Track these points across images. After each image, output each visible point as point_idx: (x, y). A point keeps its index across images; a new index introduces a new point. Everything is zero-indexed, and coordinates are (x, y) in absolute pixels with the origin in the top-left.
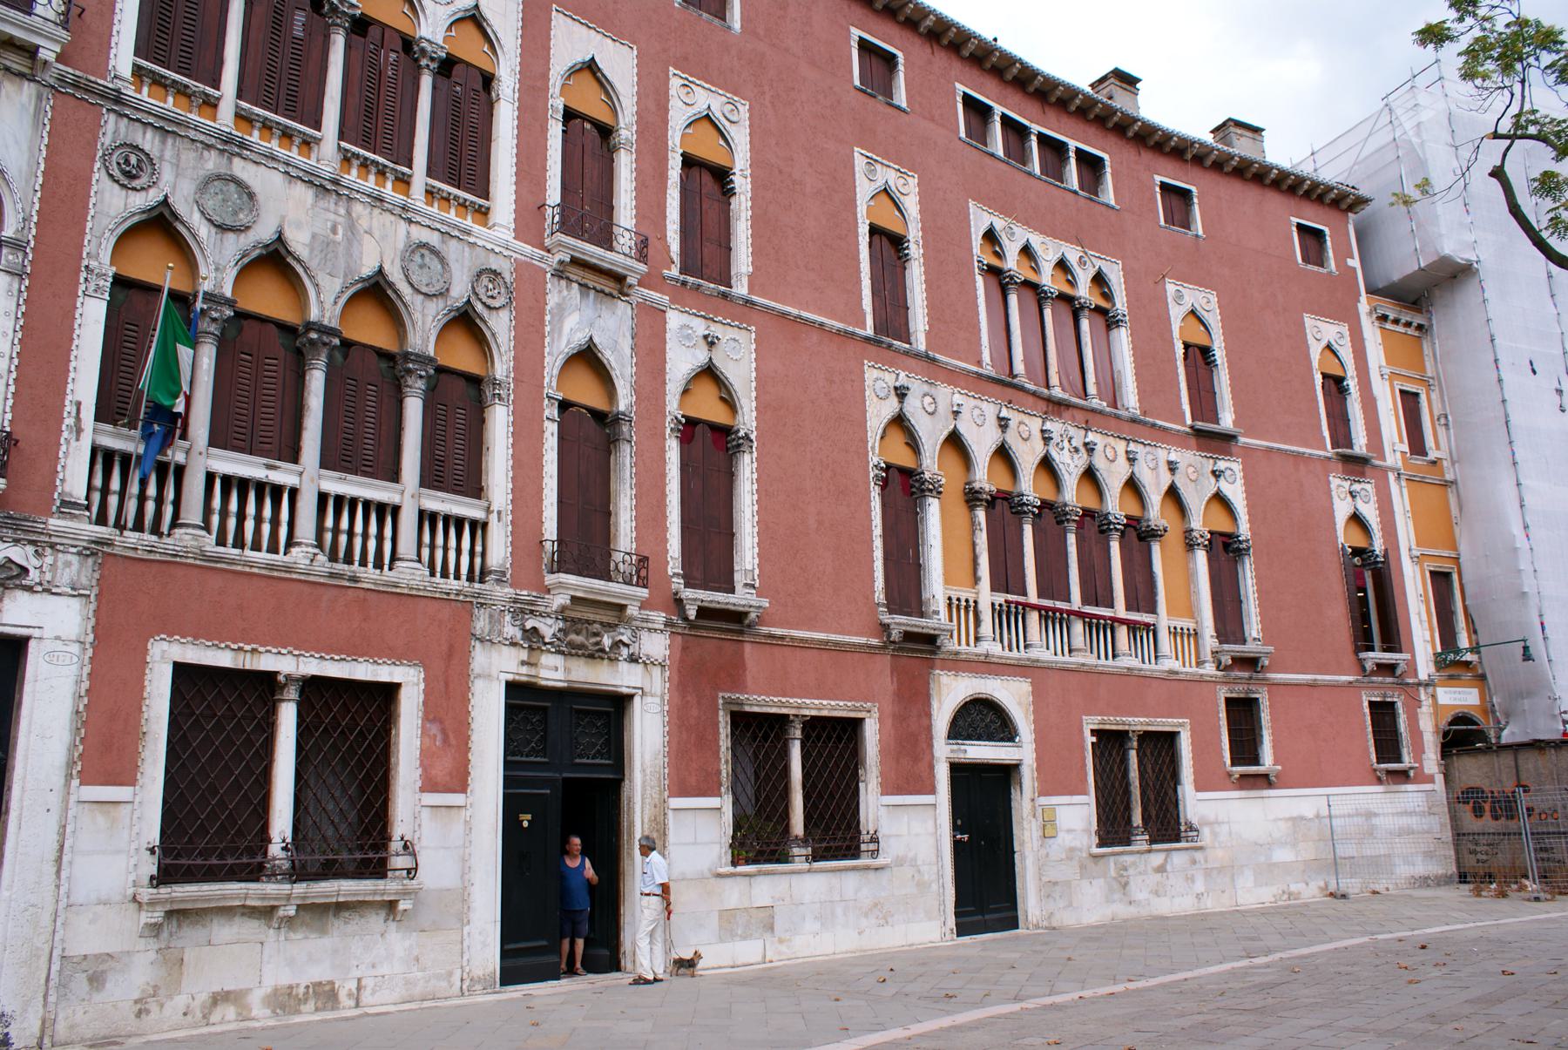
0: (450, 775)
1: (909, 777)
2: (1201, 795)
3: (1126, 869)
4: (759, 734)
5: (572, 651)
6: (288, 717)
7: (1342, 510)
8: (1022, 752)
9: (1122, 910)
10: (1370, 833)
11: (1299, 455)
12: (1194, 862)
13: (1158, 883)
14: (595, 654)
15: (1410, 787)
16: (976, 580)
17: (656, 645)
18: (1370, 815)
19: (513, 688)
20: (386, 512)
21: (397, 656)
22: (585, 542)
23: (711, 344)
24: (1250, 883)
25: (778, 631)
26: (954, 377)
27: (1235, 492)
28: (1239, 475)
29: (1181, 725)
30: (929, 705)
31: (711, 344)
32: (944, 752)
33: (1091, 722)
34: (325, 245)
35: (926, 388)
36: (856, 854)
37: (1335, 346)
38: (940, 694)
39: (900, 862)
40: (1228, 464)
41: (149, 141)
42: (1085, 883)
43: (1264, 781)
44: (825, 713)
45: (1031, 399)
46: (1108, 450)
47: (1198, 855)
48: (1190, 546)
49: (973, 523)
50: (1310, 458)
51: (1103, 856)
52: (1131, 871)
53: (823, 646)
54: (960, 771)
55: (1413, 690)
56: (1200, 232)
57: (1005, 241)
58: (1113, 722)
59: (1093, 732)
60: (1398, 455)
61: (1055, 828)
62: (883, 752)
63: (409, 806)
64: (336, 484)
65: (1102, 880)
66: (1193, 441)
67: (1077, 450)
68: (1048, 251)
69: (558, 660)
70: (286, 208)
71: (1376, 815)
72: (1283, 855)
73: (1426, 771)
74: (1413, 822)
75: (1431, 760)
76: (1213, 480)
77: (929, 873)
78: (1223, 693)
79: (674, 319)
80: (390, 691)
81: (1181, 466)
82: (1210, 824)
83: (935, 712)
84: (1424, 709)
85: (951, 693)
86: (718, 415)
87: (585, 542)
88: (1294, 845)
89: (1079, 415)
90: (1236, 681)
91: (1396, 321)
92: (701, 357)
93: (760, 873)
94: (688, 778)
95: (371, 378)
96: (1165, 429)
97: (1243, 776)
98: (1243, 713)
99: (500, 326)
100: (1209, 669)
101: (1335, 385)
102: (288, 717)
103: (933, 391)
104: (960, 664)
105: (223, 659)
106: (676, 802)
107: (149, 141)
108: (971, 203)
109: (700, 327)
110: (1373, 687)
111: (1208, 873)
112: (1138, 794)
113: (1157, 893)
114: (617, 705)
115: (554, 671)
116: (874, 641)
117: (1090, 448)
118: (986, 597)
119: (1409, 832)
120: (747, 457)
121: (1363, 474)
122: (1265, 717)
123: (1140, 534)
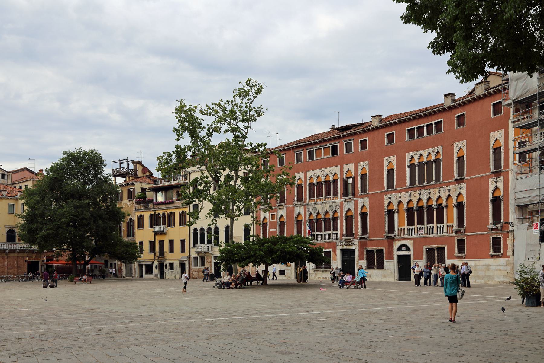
0: (335, 259)
1: (391, 257)
4: (370, 253)
5: (347, 245)
7: (492, 187)
8: (411, 253)
14: (349, 245)
17: (357, 243)
20: (330, 234)
21: (330, 248)
22: (349, 233)
26: (400, 191)
32: (396, 253)
34: (322, 210)
41: (309, 207)
50: (484, 176)
54: (399, 257)
57: (415, 157)
58: (430, 246)
64: (326, 233)
68: (424, 153)
70: (319, 208)
79: (359, 200)
85: (397, 244)
87: (349, 233)
89: (428, 187)
90: (459, 236)
91: (523, 119)
95: (326, 220)
98: (461, 243)
99: (338, 211)
100: (453, 234)
104: (398, 240)
107: (309, 207)
109: (362, 200)
114: (353, 251)
115: (345, 247)
118: (406, 227)
123: (440, 208)
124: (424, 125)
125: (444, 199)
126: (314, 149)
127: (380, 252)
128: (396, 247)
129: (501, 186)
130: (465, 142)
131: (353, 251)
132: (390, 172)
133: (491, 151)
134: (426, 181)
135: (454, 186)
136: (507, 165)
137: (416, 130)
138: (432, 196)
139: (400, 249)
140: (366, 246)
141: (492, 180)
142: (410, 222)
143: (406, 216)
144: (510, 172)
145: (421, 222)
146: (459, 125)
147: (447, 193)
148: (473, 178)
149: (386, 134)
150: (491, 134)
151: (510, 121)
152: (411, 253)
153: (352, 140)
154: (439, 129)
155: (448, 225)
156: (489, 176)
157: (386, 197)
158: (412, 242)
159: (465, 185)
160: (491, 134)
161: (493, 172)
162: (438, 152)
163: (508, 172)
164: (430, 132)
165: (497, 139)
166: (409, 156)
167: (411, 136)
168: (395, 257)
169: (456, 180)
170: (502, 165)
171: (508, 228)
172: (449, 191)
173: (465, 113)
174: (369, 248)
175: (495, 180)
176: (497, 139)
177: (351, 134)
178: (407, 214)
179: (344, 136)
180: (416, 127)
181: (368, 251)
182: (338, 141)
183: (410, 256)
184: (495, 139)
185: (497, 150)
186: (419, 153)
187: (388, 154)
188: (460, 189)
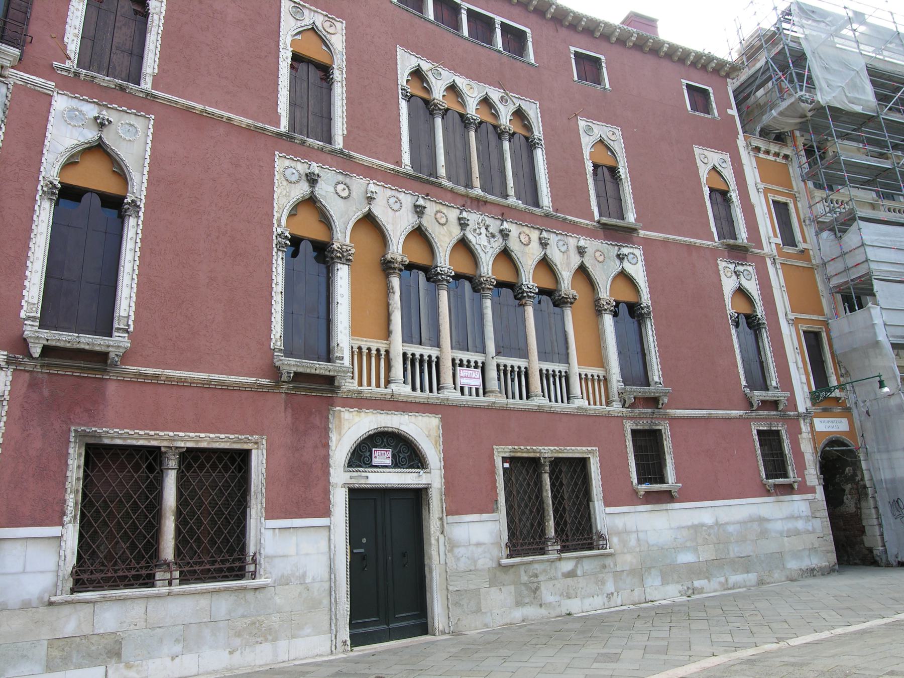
2: (609, 510)
3: (536, 576)
7: (729, 285)
8: (432, 478)
9: (531, 612)
10: (764, 534)
12: (604, 567)
13: (567, 586)
15: (795, 497)
16: (388, 334)
18: (762, 520)
23: (102, 125)
24: (657, 582)
25: (150, 371)
26: (369, 172)
27: (638, 271)
28: (641, 258)
29: (590, 452)
30: (327, 437)
31: (102, 125)
32: (341, 479)
33: (501, 452)
35: (340, 178)
36: (238, 573)
37: (719, 168)
38: (339, 428)
39: (284, 581)
40: (631, 250)
42: (494, 590)
43: (667, 497)
44: (204, 445)
45: (449, 195)
46: (522, 237)
47: (609, 561)
48: (599, 311)
49: (388, 290)
50: (699, 248)
51: (512, 566)
52: (541, 578)
53: (206, 386)
54: (359, 497)
55: (794, 422)
56: (608, 86)
58: (525, 451)
59: (504, 459)
60: (773, 246)
61: (466, 542)
62: (271, 478)
65: (512, 588)
66: (601, 232)
67: (493, 236)
71: (768, 520)
72: (686, 558)
73: (808, 484)
74: (800, 525)
75: (813, 476)
76: (618, 262)
77: (319, 589)
78: (629, 426)
79: (61, 103)
81: (590, 251)
82: (618, 533)
83: (333, 444)
84: (804, 435)
85: (351, 427)
86: (103, 182)
88: (695, 550)
92: (90, 135)
93: (104, 600)
97: (647, 493)
100: (616, 407)
101: (721, 196)
103: (348, 181)
104: (360, 402)
108: (400, 51)
109: (91, 110)
110: (758, 419)
111: (617, 575)
112: (550, 509)
113: (569, 597)
116: (264, 381)
117: (505, 234)
118: (398, 347)
119: (797, 533)
120: (132, 222)
121: (745, 259)
122: (668, 444)
128: (341, 447)
139: (360, 457)
140: (93, 417)
148: (665, 242)
152: (432, 478)
158: (432, 422)
168: (339, 500)
174: (118, 435)
181: (97, 454)
188: (621, 257)
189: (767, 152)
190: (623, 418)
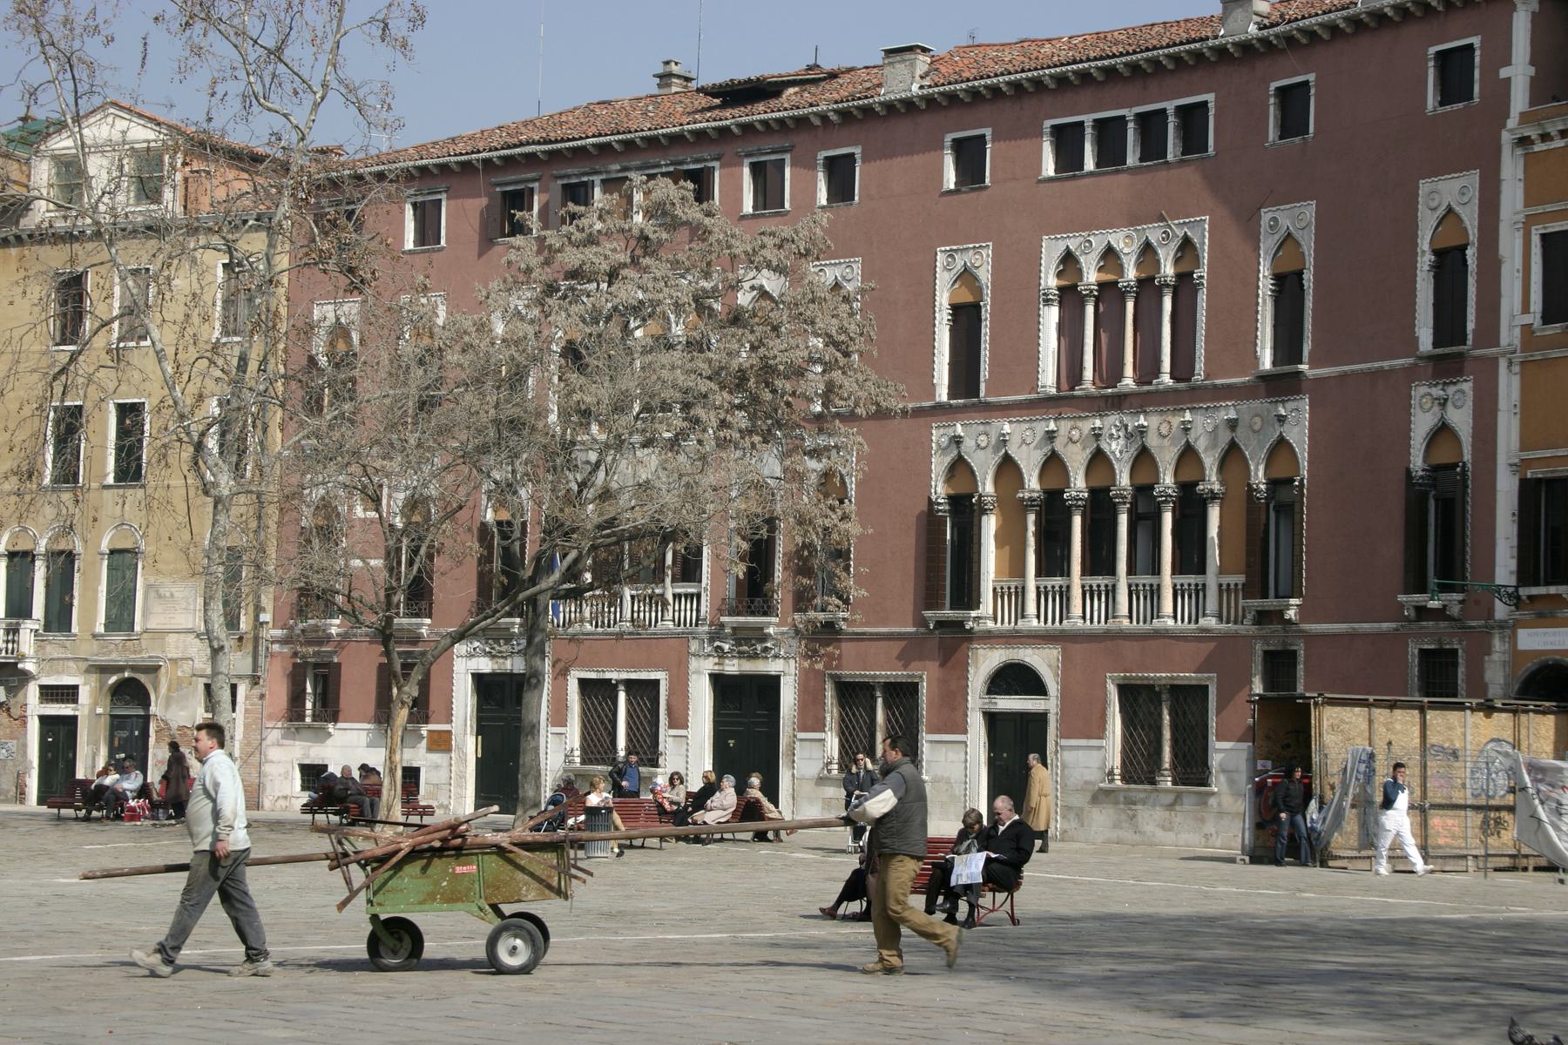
0: (679, 721)
4: (853, 695)
6: (622, 696)
7: (1422, 424)
8: (1049, 704)
11: (1380, 371)
14: (754, 656)
19: (711, 675)
26: (1005, 409)
27: (1299, 436)
32: (976, 701)
35: (981, 428)
38: (976, 662)
50: (1392, 370)
54: (992, 719)
60: (1517, 331)
63: (666, 736)
66: (1262, 385)
68: (1125, 242)
69: (735, 661)
78: (1259, 647)
80: (657, 682)
84: (1495, 657)
94: (810, 720)
96: (1229, 386)
100: (1247, 628)
102: (622, 696)
104: (990, 638)
105: (593, 675)
106: (801, 735)
113: (1163, 827)
114: (773, 683)
115: (732, 667)
124: (1128, 113)
125: (1210, 462)
126: (597, 179)
127: (902, 694)
129: (1461, 419)
130: (1309, 210)
131: (770, 685)
132: (966, 317)
133: (1425, 260)
134: (1129, 370)
135: (1256, 404)
136: (1490, 333)
137: (1089, 131)
138: (1152, 441)
141: (1423, 390)
142: (1053, 561)
143: (1031, 528)
144: (1503, 363)
145: (1099, 560)
146: (1285, 132)
147: (1225, 437)
148: (1344, 375)
149: (949, 138)
150: (1424, 186)
151: (1506, 137)
153: (784, 151)
154: (1193, 139)
155: (1226, 580)
156: (1411, 374)
157: (939, 436)
159: (1305, 404)
160: (1424, 186)
161: (1430, 358)
162: (1187, 244)
163: (1494, 361)
164: (1153, 149)
165: (1450, 210)
166: (1051, 252)
167: (1069, 159)
169: (1265, 378)
170: (1471, 326)
171: (1490, 612)
172: (1233, 425)
173: (1311, 77)
174: (851, 673)
175: (1437, 392)
176: (1450, 210)
177: (781, 121)
178: (1038, 523)
179: (747, 128)
180: (1088, 119)
182: (715, 151)
183: (1041, 719)
184: (1441, 212)
185: (1449, 262)
186: (1098, 242)
187: (959, 236)
189: (1545, 137)
190: (1254, 637)
